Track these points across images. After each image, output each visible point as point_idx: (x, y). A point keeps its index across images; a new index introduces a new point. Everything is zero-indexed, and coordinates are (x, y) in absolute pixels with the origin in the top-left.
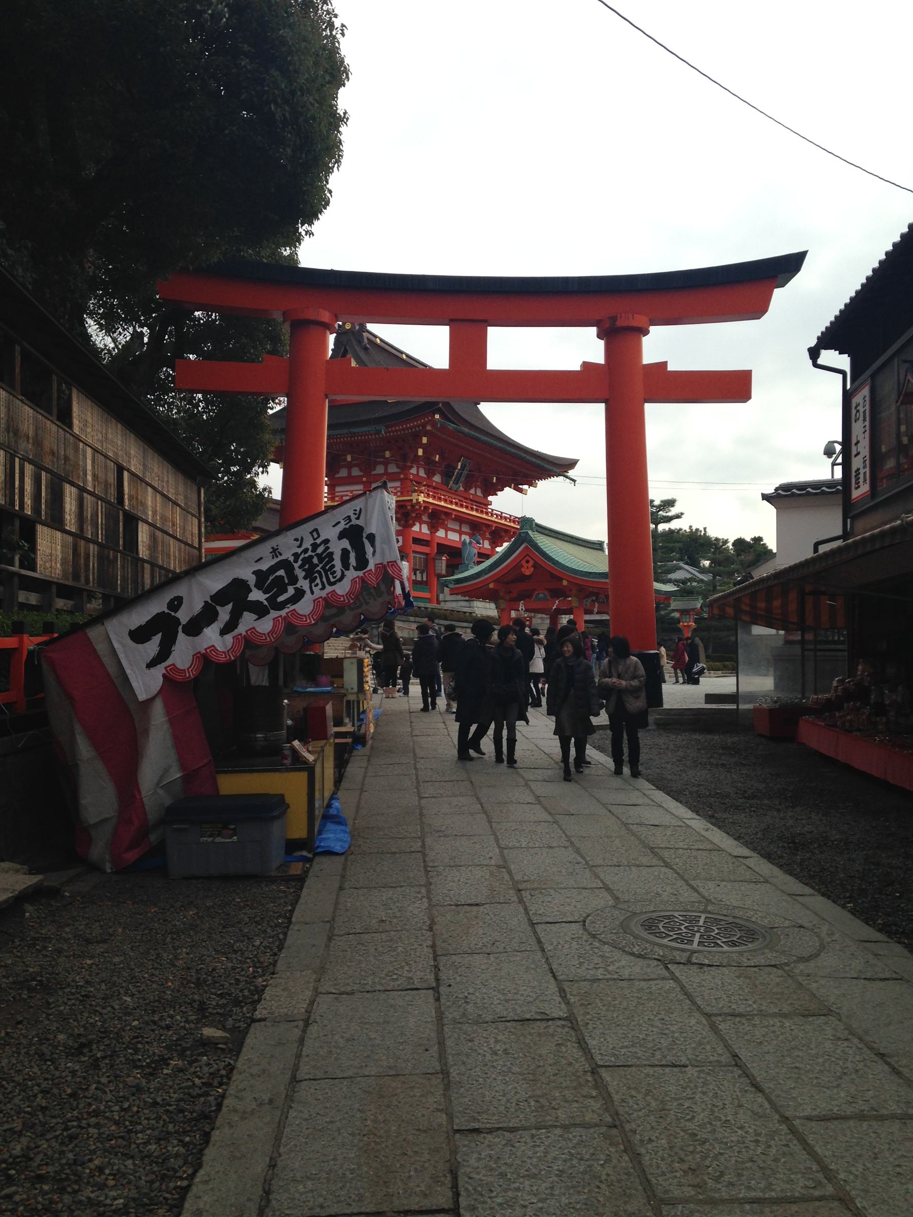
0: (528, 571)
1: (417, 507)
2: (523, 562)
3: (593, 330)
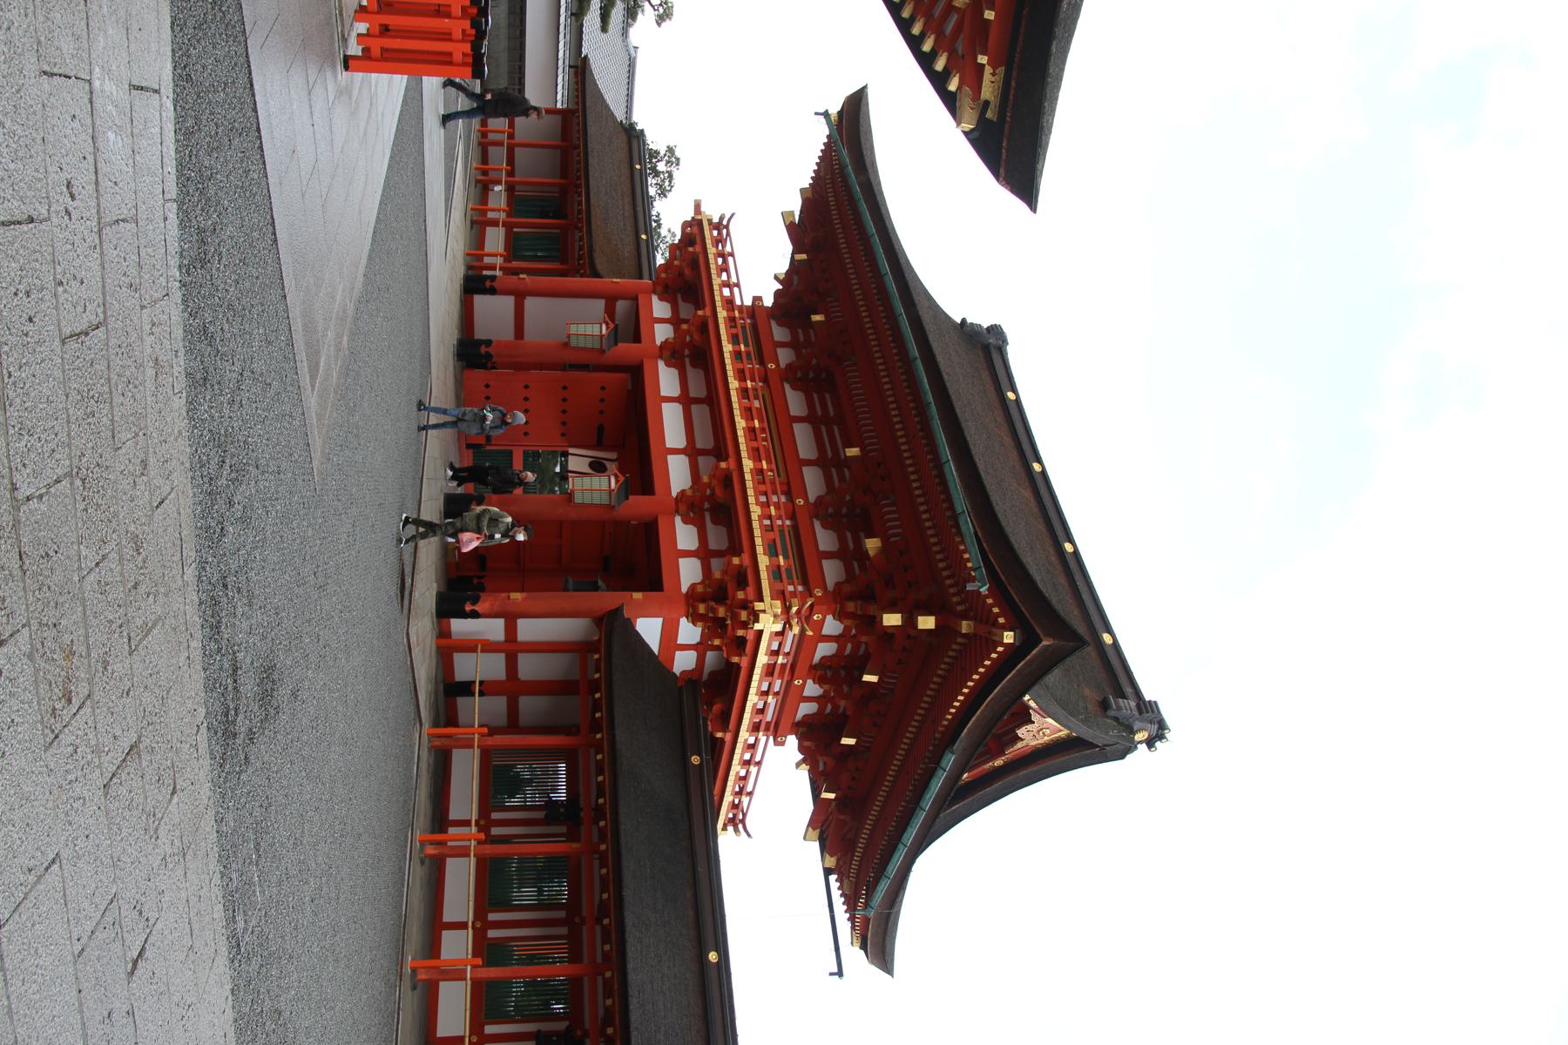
1: (744, 615)
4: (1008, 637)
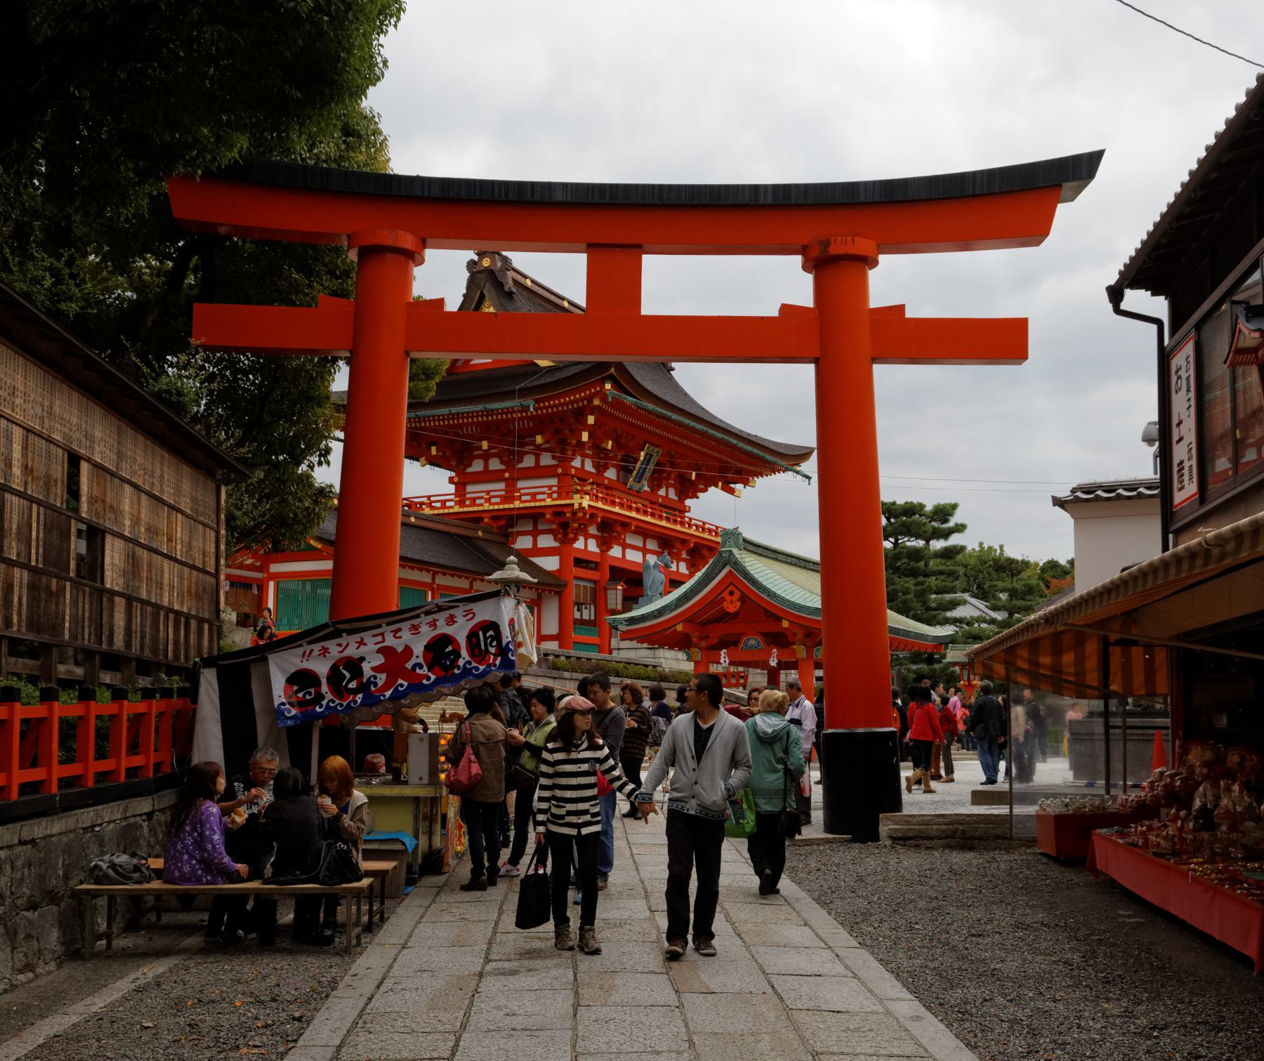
0: (732, 606)
1: (580, 514)
2: (726, 595)
3: (798, 259)
4: (608, 386)
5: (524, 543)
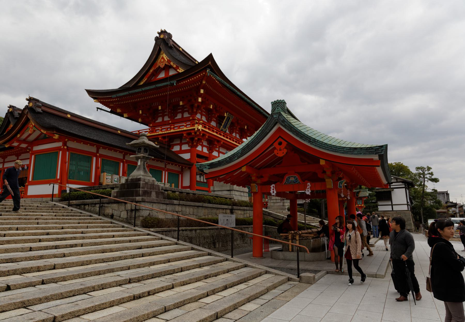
0: (281, 152)
1: (198, 133)
5: (176, 148)
